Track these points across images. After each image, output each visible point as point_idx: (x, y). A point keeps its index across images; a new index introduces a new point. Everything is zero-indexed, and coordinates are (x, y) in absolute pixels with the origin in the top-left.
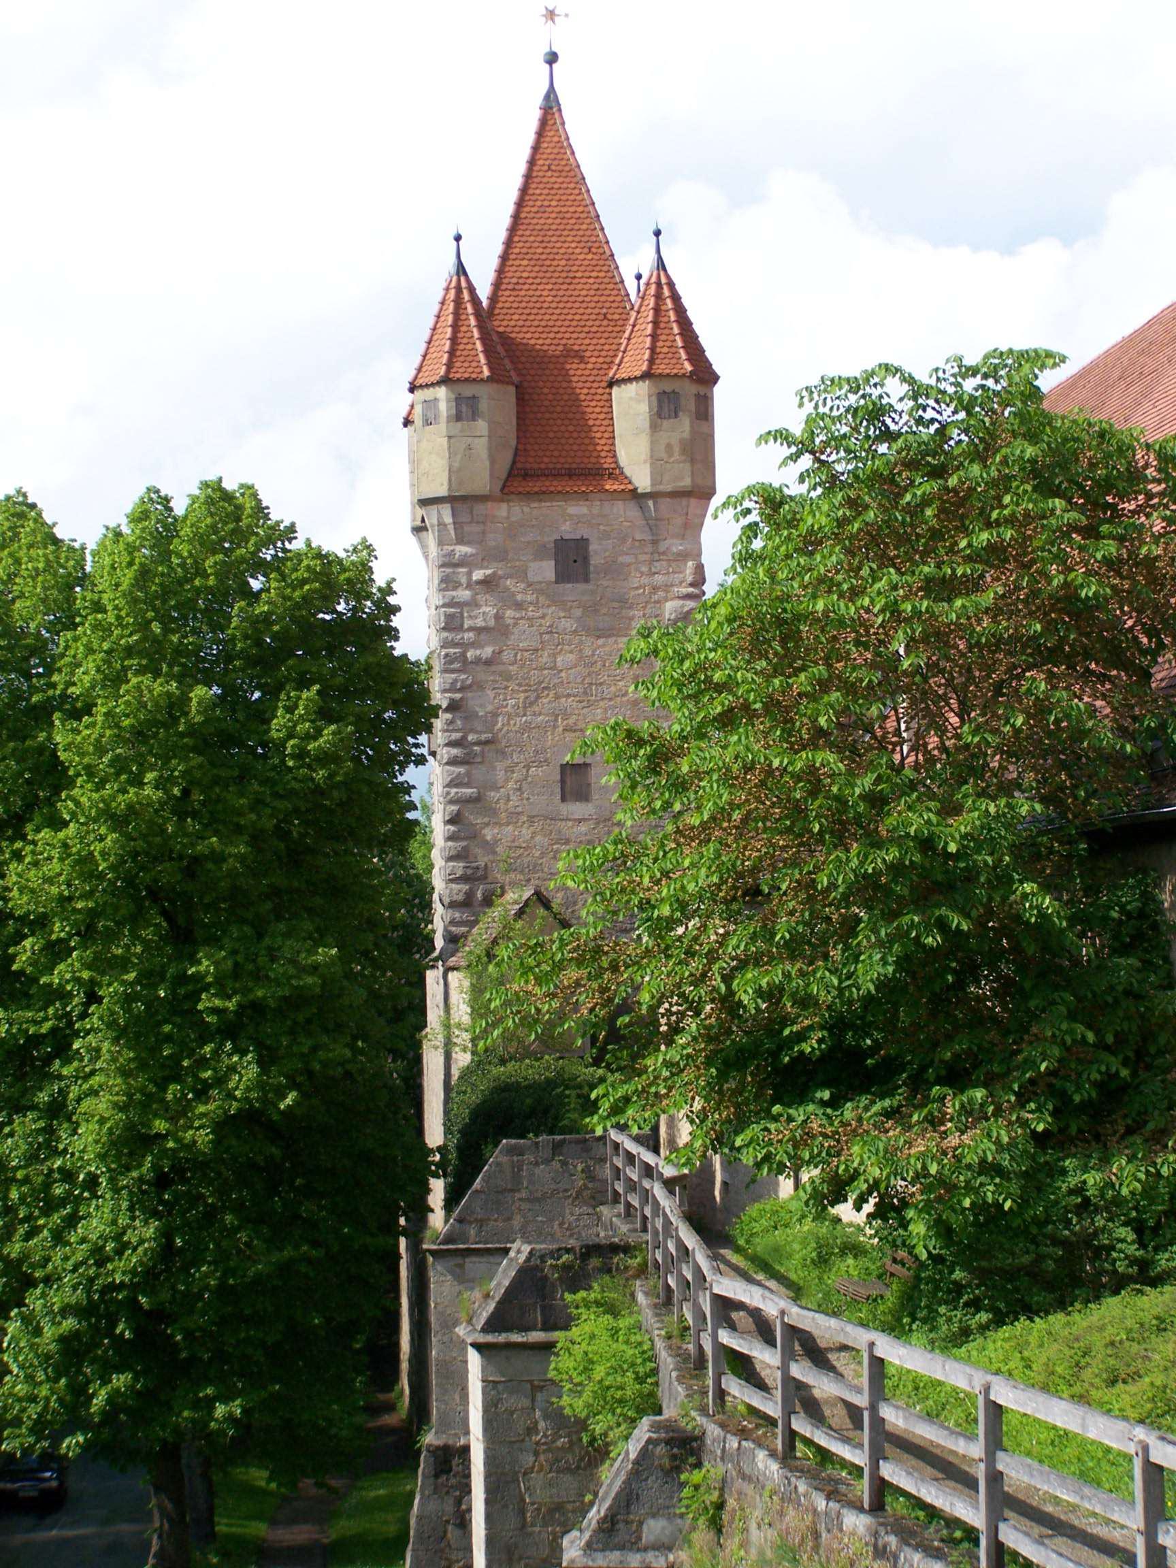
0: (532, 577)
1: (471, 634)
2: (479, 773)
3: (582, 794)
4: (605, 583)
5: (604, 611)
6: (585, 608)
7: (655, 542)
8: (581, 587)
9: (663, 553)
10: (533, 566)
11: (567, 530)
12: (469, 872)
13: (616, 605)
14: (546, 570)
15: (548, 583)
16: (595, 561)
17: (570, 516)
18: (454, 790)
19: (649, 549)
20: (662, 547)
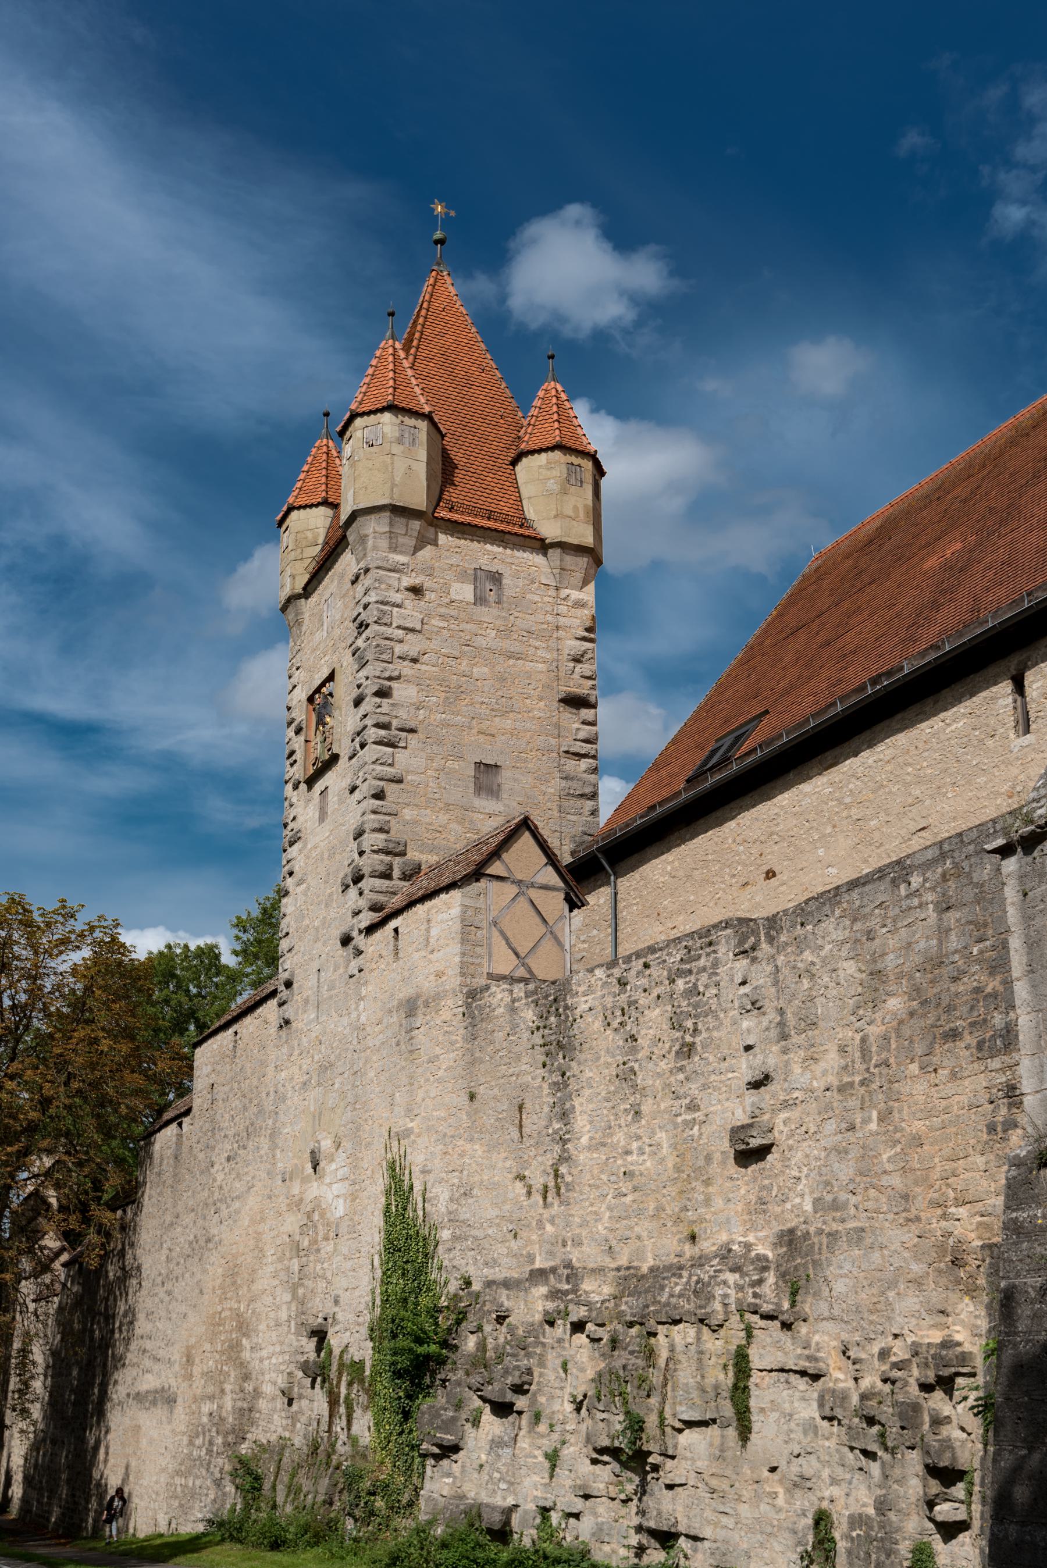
0: (454, 595)
1: (401, 632)
2: (400, 756)
3: (493, 792)
4: (516, 614)
5: (515, 636)
6: (499, 631)
7: (557, 589)
8: (495, 611)
9: (564, 599)
10: (456, 587)
11: (484, 562)
12: (391, 845)
13: (525, 634)
14: (465, 592)
15: (468, 603)
16: (508, 592)
17: (488, 555)
18: (379, 768)
19: (552, 592)
20: (564, 593)
